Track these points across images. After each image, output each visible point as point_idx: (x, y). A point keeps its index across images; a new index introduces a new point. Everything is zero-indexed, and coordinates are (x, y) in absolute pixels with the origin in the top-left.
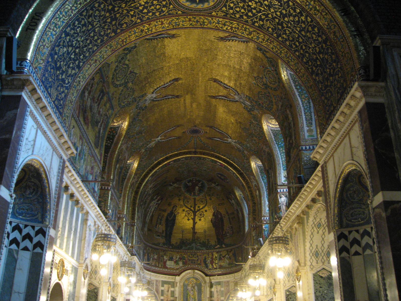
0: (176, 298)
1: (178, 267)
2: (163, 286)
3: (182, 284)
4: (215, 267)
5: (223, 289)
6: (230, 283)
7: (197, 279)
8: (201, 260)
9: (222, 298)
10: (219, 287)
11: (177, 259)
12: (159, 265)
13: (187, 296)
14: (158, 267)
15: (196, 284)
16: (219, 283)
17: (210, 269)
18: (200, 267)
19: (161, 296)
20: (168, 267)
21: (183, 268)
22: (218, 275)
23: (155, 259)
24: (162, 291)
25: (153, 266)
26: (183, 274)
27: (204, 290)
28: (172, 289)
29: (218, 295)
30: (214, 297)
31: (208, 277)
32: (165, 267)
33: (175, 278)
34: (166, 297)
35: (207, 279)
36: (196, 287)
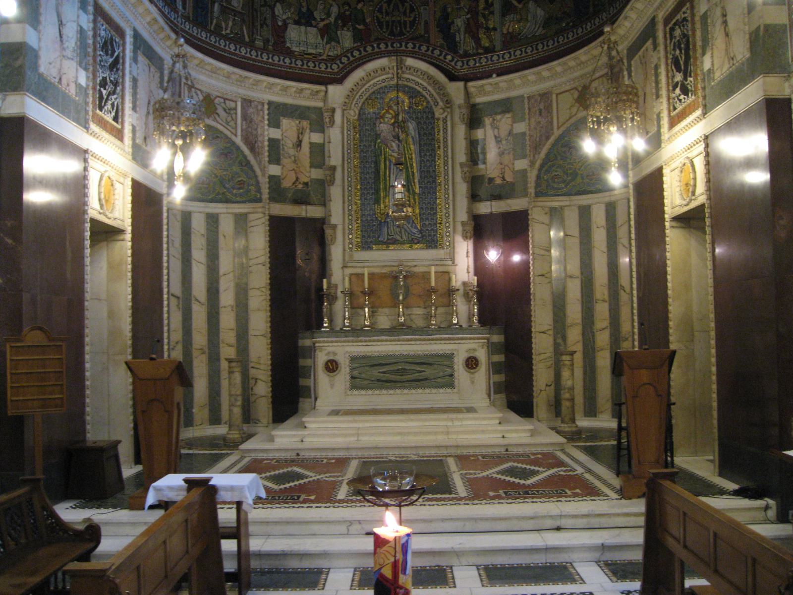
0: (333, 169)
1: (338, 51)
2: (277, 126)
3: (353, 114)
4: (486, 43)
5: (521, 127)
6: (554, 96)
7: (413, 93)
8: (426, 23)
9: (521, 164)
10: (505, 122)
11: (332, 19)
12: (253, 41)
13: (377, 163)
14: (251, 45)
15: (411, 111)
16: (505, 106)
17: (466, 55)
18: (424, 48)
19: (270, 162)
20: (294, 49)
21: (356, 53)
22: (498, 75)
23: (235, 13)
24: (274, 144)
25: (226, 38)
26: (358, 75)
27: (445, 132)
28: (316, 138)
29: (501, 154)
30: (484, 163)
31: (461, 84)
32: (280, 46)
33: (326, 92)
34: (294, 166)
35: (456, 89)
36: (411, 126)
